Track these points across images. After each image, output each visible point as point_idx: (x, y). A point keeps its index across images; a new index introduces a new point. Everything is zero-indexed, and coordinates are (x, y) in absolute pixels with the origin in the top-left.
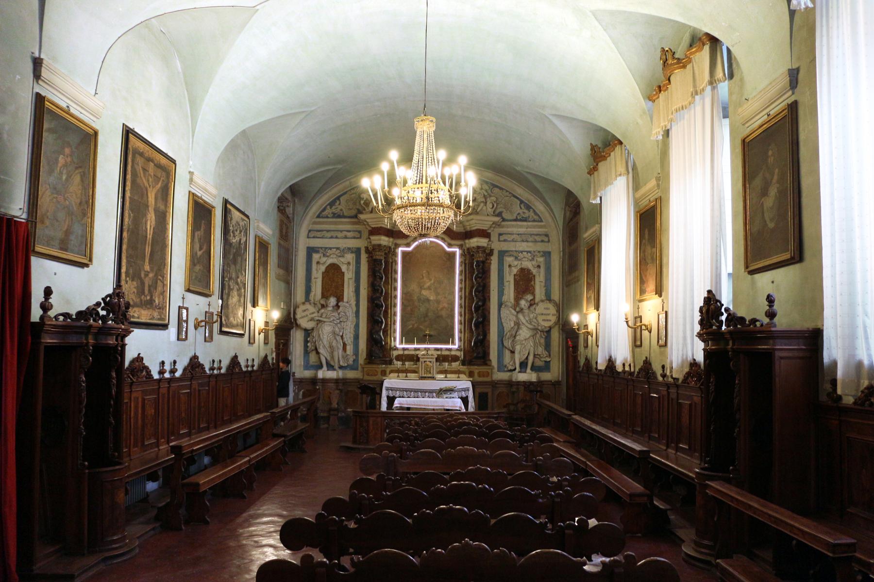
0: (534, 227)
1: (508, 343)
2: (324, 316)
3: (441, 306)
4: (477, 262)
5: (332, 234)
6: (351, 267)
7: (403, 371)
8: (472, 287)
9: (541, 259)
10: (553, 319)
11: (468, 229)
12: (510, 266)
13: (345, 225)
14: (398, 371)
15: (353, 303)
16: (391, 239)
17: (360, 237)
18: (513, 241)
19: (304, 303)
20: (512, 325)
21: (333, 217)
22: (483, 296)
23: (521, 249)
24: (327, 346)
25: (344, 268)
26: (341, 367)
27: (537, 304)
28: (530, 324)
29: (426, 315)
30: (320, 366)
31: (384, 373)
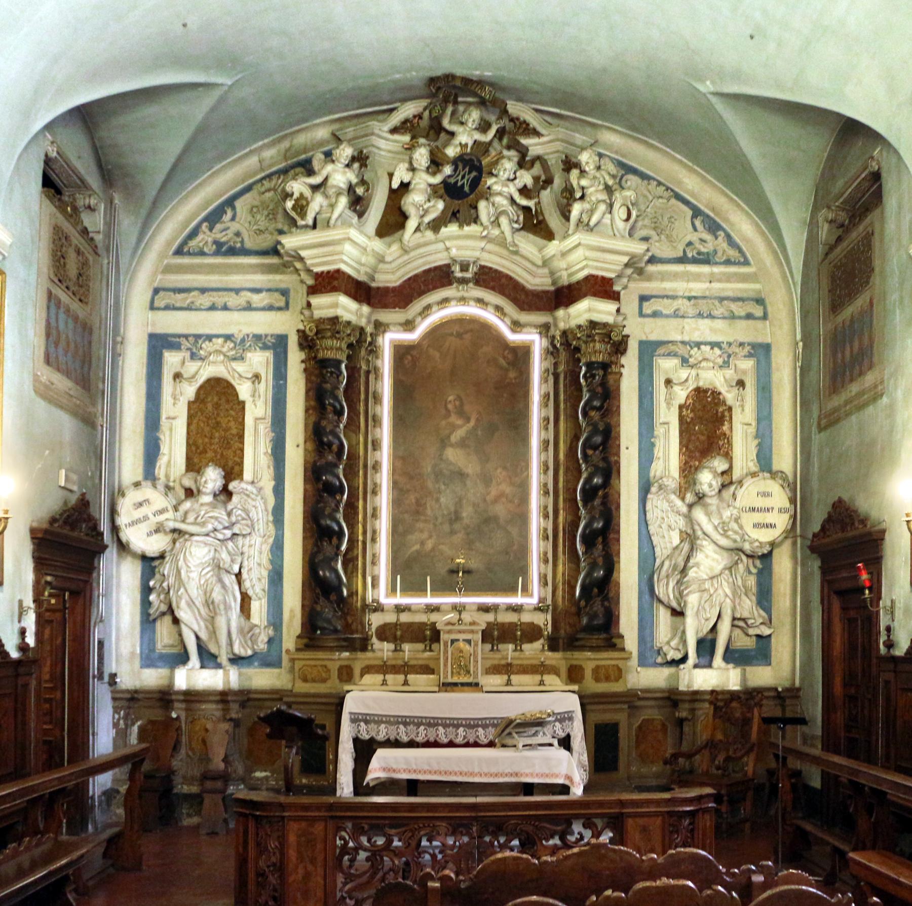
0: (728, 278)
1: (666, 590)
2: (191, 518)
3: (494, 492)
4: (590, 365)
5: (219, 299)
6: (262, 387)
7: (395, 669)
8: (576, 438)
9: (748, 365)
10: (782, 521)
11: (565, 280)
12: (668, 382)
13: (248, 275)
14: (384, 668)
15: (268, 484)
16: (366, 309)
17: (287, 307)
18: (676, 315)
19: (137, 485)
20: (676, 541)
21: (217, 253)
22: (605, 459)
23: (696, 337)
24: (199, 602)
25: (244, 391)
26: (236, 660)
27: (740, 483)
28: (725, 534)
29: (456, 517)
30: (182, 658)
31: (346, 674)
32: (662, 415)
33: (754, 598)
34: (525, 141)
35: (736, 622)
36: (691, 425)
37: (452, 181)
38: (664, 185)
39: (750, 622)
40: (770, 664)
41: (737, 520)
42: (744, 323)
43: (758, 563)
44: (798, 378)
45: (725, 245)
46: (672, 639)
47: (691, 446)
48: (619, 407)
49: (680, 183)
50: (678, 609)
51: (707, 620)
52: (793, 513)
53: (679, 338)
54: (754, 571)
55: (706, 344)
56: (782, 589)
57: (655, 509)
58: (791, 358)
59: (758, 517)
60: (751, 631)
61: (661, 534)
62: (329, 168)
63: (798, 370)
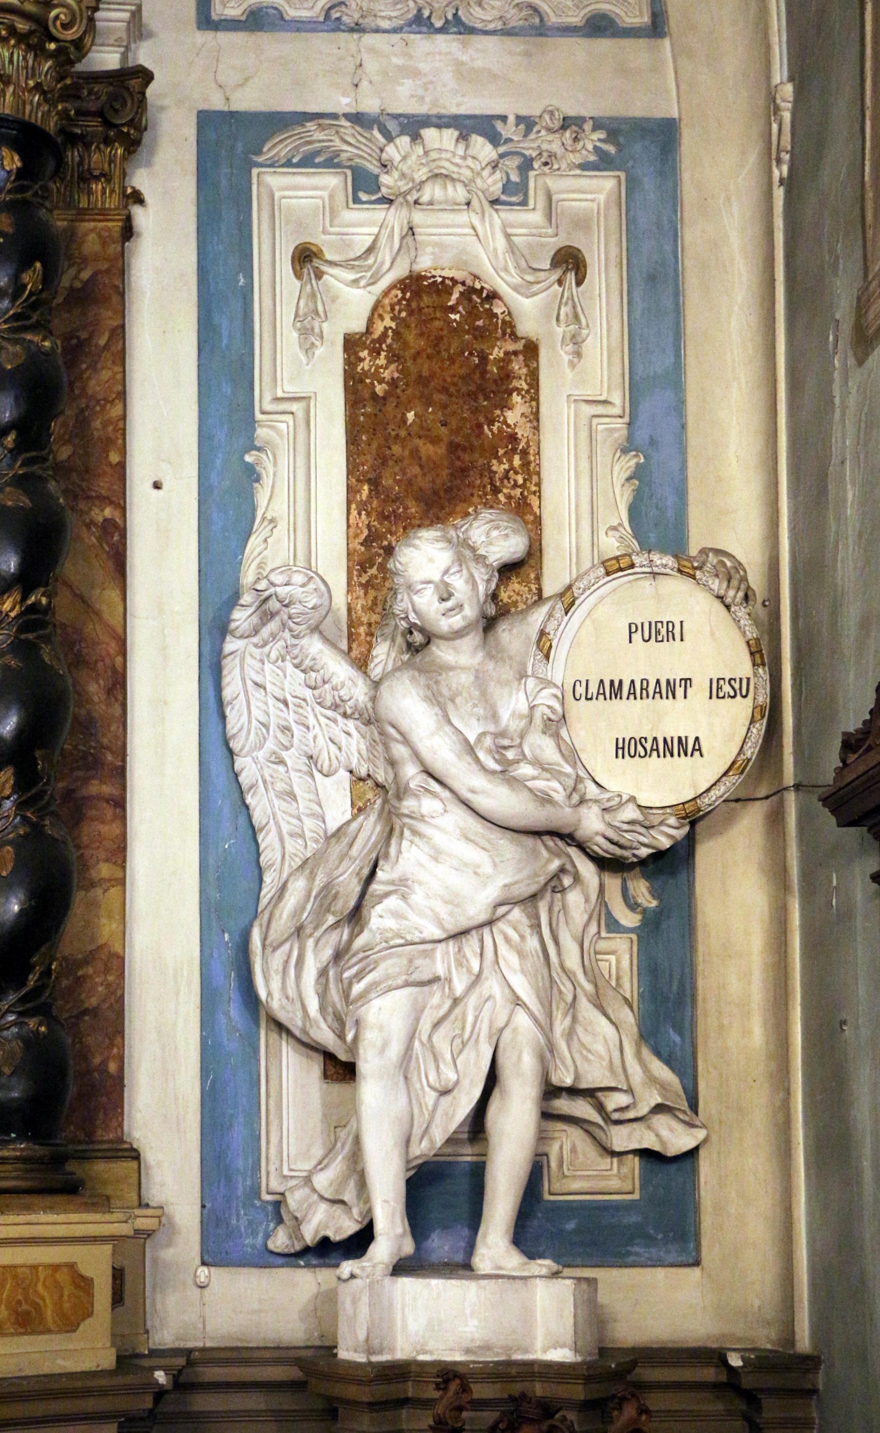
9: (592, 195)
10: (724, 731)
12: (305, 257)
20: (338, 809)
23: (405, 99)
27: (568, 599)
28: (505, 774)
32: (285, 369)
33: (628, 1018)
35: (563, 1105)
36: (391, 404)
39: (614, 1101)
40: (697, 1263)
41: (555, 725)
42: (579, 49)
43: (641, 889)
44: (779, 223)
46: (321, 1165)
47: (387, 481)
48: (119, 333)
50: (343, 1057)
51: (445, 1092)
52: (764, 698)
53: (344, 103)
54: (629, 919)
55: (441, 122)
56: (734, 986)
57: (256, 695)
58: (753, 157)
59: (634, 718)
60: (622, 1138)
61: (280, 786)
63: (779, 194)
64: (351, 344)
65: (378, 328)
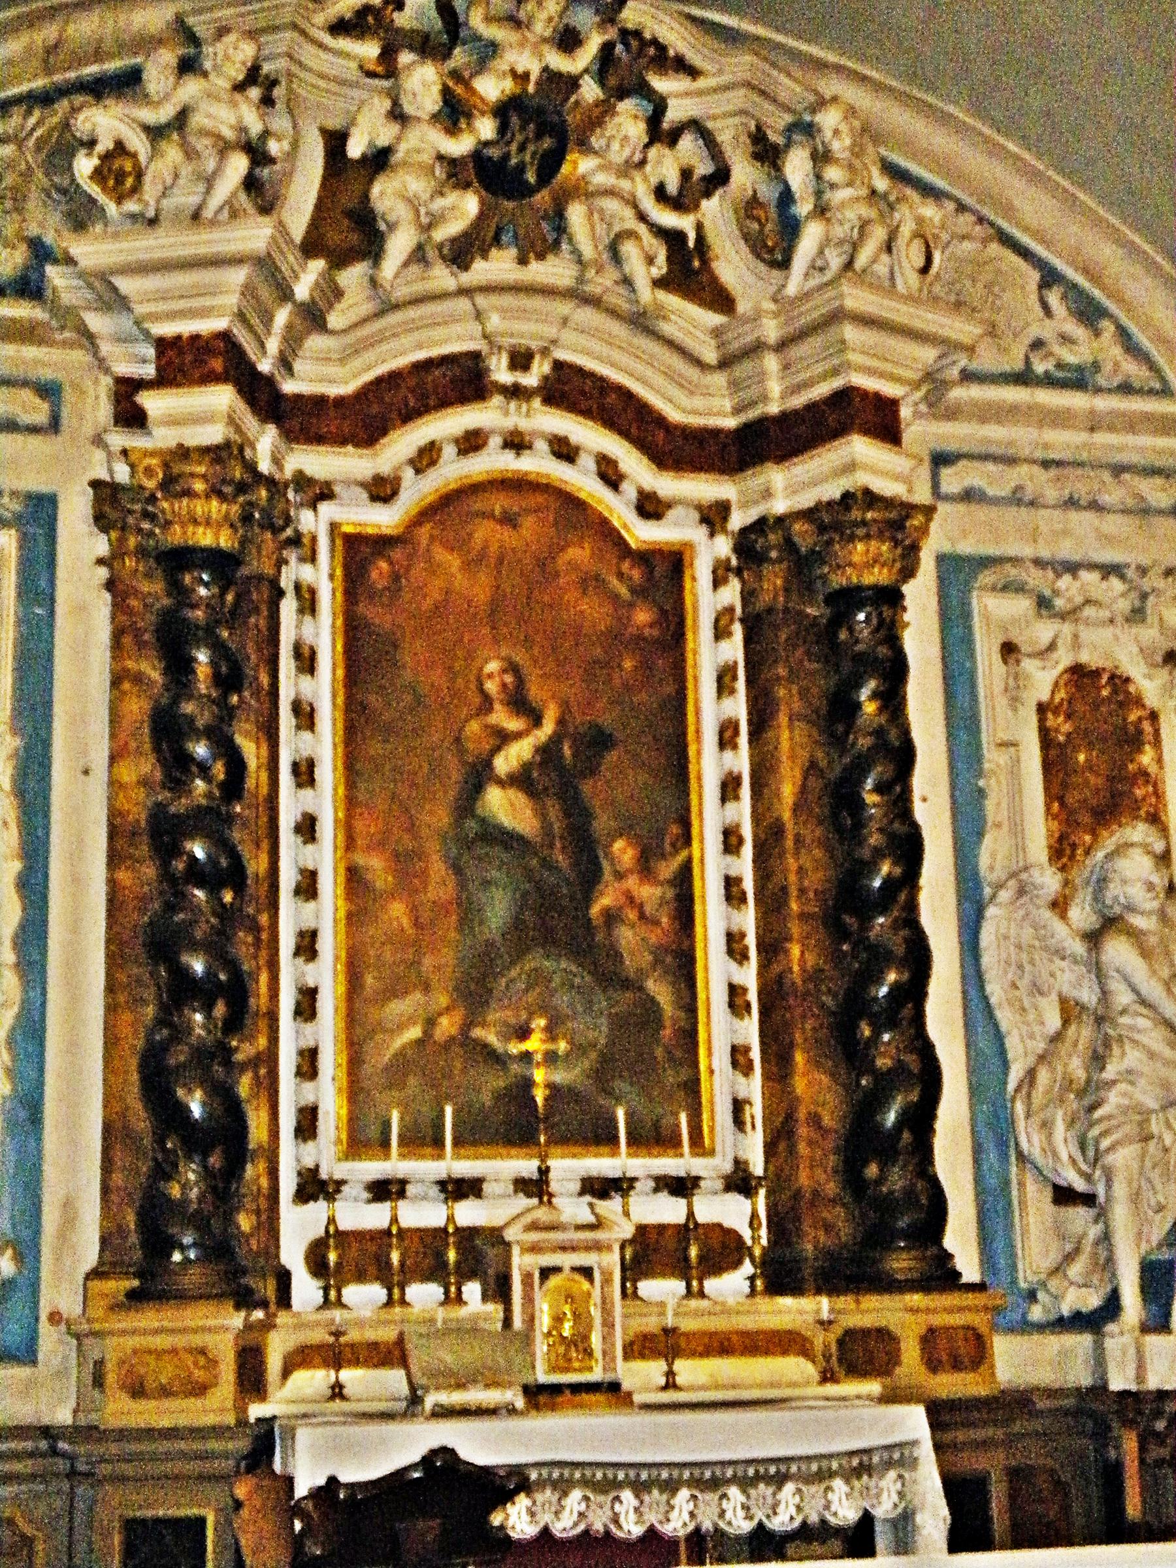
1: (1046, 1140)
18: (1017, 499)
23: (1067, 550)
34: (660, 84)
37: (494, 153)
38: (973, 212)
45: (1117, 351)
47: (1070, 800)
49: (1008, 210)
53: (1027, 551)
55: (1092, 566)
62: (191, 88)
64: (1042, 709)
65: (1057, 700)
